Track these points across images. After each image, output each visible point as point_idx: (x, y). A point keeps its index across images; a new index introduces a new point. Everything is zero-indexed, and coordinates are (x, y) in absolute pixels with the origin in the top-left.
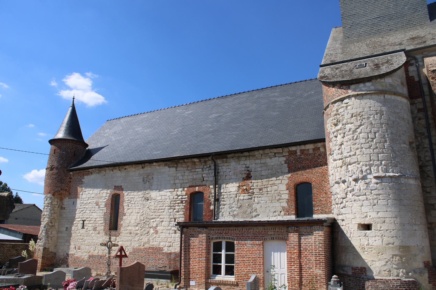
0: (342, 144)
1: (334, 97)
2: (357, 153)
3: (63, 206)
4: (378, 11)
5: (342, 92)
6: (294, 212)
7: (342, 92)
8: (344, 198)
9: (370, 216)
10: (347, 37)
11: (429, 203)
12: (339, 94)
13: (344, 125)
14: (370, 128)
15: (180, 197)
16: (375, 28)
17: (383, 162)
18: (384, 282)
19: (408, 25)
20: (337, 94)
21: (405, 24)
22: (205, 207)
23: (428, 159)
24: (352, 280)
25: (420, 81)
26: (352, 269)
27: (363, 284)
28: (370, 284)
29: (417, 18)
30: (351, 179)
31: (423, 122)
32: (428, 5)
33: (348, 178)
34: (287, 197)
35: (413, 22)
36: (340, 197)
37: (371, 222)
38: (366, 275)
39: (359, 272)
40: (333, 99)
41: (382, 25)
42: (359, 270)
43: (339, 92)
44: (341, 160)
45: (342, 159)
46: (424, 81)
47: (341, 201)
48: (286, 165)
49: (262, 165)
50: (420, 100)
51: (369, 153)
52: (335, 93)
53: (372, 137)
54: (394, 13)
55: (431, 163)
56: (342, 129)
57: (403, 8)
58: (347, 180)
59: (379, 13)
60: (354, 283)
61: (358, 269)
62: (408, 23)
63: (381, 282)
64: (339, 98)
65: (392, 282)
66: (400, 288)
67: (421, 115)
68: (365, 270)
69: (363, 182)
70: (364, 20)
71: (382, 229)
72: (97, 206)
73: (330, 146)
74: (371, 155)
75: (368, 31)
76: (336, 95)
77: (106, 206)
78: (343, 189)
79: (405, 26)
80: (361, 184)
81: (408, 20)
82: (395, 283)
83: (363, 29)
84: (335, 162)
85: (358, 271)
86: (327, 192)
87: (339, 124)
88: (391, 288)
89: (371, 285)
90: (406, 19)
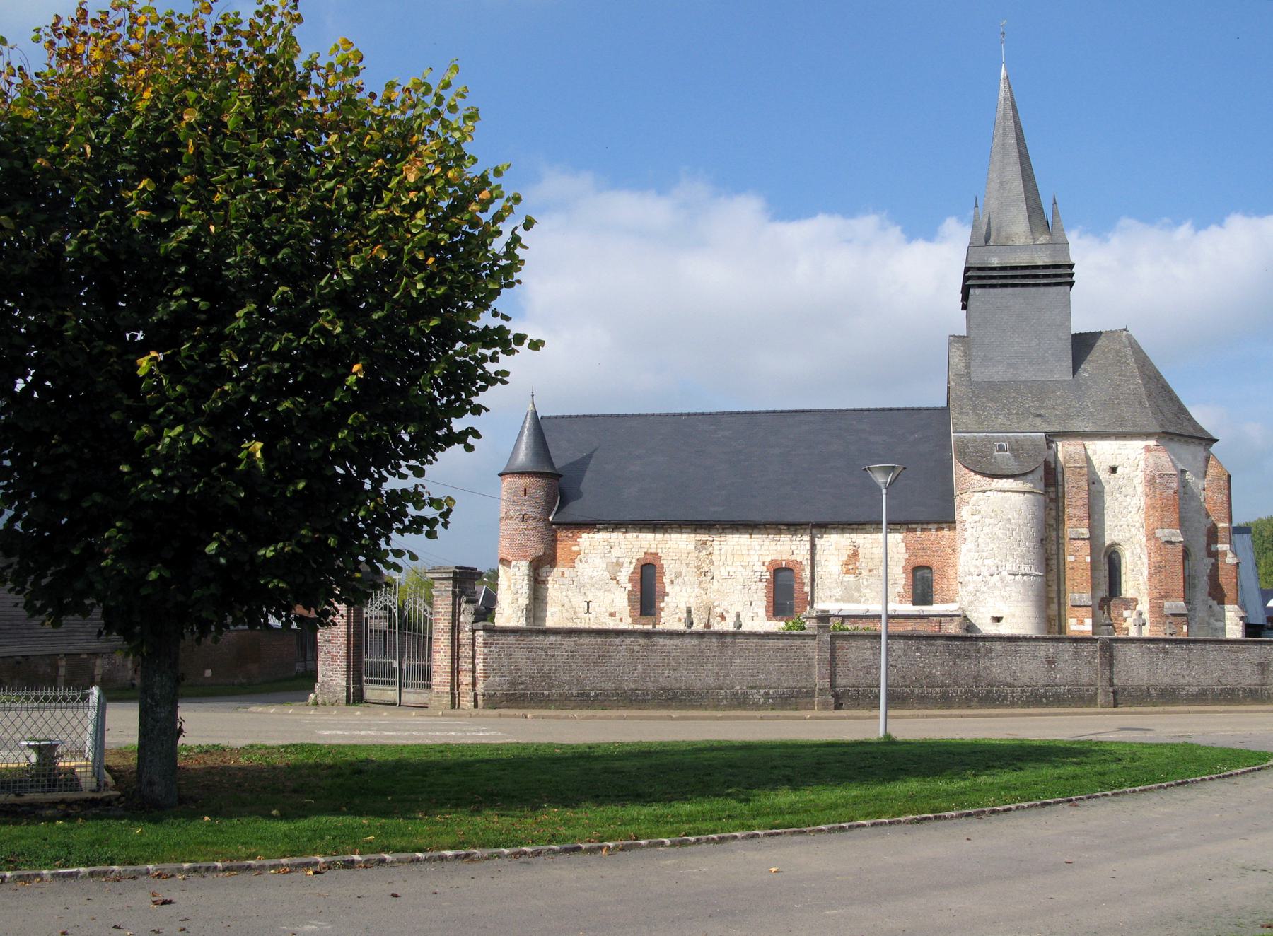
3: (540, 579)
6: (911, 599)
15: (759, 573)
22: (796, 587)
23: (1053, 552)
25: (1055, 469)
31: (1053, 513)
32: (1075, 336)
34: (903, 582)
46: (1059, 469)
48: (903, 544)
49: (873, 541)
50: (1053, 489)
55: (1055, 556)
57: (1046, 352)
64: (981, 489)
67: (1052, 505)
72: (615, 582)
77: (630, 580)
80: (996, 578)
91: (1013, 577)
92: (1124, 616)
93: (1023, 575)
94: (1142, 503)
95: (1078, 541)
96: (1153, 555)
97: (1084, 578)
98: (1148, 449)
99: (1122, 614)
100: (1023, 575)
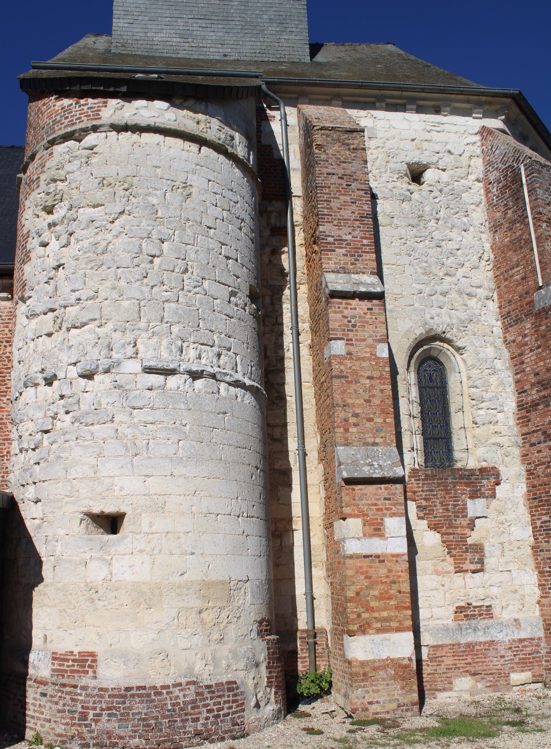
0: (59, 266)
1: (56, 128)
2: (102, 294)
4: (202, 5)
5: (80, 114)
7: (80, 114)
8: (47, 432)
9: (122, 489)
10: (120, 45)
11: (277, 467)
12: (72, 120)
13: (74, 210)
14: (148, 225)
16: (190, 40)
17: (175, 329)
18: (149, 695)
19: (264, 55)
20: (67, 118)
21: (259, 51)
24: (52, 696)
26: (54, 659)
27: (83, 707)
28: (104, 706)
29: (285, 44)
30: (73, 372)
33: (65, 370)
35: (276, 52)
36: (36, 430)
37: (123, 510)
38: (95, 678)
39: (75, 668)
40: (52, 134)
41: (207, 37)
42: (74, 661)
43: (73, 113)
44: (50, 315)
45: (53, 310)
47: (36, 441)
51: (138, 295)
52: (61, 117)
53: (153, 253)
54: (238, 19)
56: (66, 221)
58: (61, 375)
59: (205, 9)
60: (57, 703)
61: (73, 657)
62: (266, 51)
63: (139, 696)
65: (171, 692)
66: (193, 708)
68: (95, 661)
69: (108, 378)
70: (167, 15)
71: (154, 529)
73: (23, 275)
74: (142, 304)
75: (174, 44)
76: (63, 121)
78: (48, 403)
79: (259, 55)
81: (265, 44)
82: (181, 694)
83: (162, 35)
84: (35, 321)
85: (70, 663)
86: (4, 424)
87: (61, 207)
88: (169, 711)
89: (109, 709)
90: (262, 40)
91: (156, 379)
92: (471, 513)
93: (195, 375)
94: (487, 246)
95: (355, 302)
96: (529, 357)
97: (376, 401)
98: (485, 132)
99: (464, 509)
100: (195, 375)
